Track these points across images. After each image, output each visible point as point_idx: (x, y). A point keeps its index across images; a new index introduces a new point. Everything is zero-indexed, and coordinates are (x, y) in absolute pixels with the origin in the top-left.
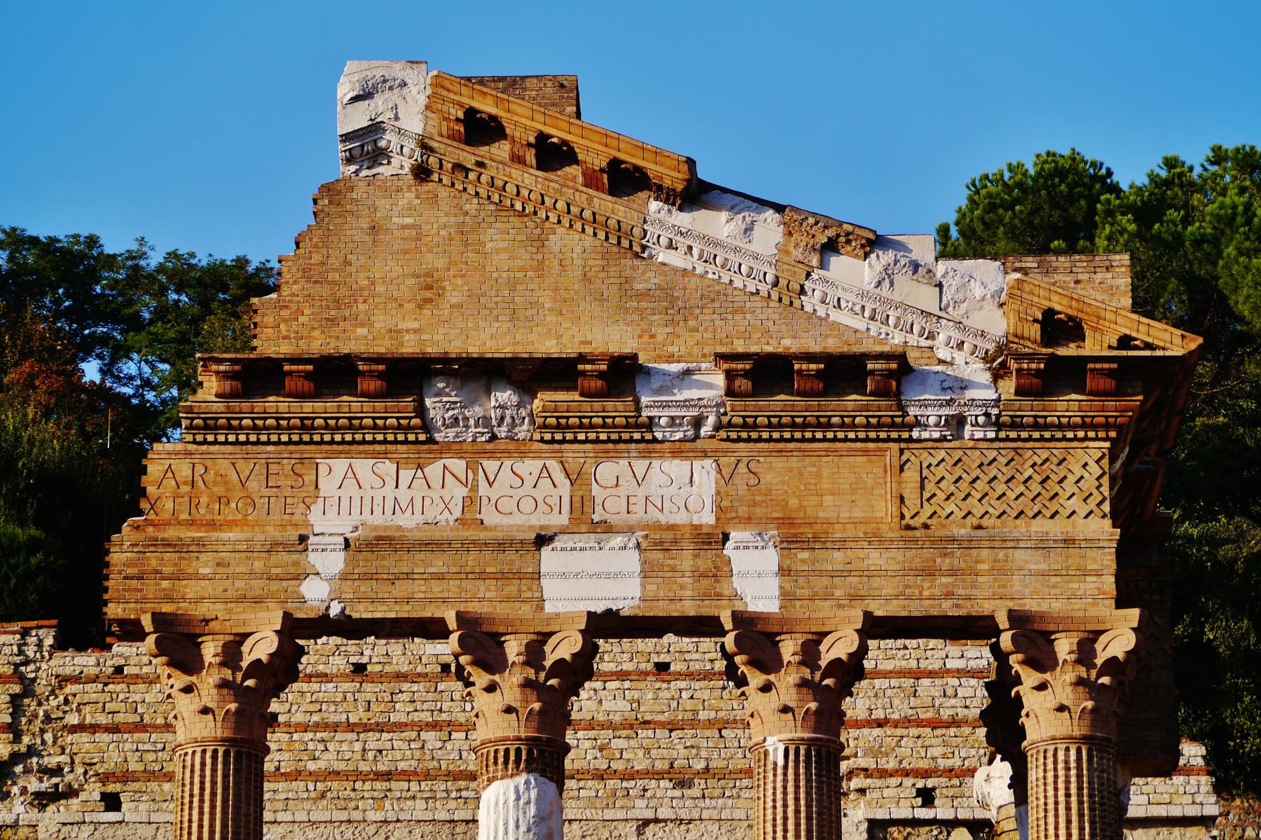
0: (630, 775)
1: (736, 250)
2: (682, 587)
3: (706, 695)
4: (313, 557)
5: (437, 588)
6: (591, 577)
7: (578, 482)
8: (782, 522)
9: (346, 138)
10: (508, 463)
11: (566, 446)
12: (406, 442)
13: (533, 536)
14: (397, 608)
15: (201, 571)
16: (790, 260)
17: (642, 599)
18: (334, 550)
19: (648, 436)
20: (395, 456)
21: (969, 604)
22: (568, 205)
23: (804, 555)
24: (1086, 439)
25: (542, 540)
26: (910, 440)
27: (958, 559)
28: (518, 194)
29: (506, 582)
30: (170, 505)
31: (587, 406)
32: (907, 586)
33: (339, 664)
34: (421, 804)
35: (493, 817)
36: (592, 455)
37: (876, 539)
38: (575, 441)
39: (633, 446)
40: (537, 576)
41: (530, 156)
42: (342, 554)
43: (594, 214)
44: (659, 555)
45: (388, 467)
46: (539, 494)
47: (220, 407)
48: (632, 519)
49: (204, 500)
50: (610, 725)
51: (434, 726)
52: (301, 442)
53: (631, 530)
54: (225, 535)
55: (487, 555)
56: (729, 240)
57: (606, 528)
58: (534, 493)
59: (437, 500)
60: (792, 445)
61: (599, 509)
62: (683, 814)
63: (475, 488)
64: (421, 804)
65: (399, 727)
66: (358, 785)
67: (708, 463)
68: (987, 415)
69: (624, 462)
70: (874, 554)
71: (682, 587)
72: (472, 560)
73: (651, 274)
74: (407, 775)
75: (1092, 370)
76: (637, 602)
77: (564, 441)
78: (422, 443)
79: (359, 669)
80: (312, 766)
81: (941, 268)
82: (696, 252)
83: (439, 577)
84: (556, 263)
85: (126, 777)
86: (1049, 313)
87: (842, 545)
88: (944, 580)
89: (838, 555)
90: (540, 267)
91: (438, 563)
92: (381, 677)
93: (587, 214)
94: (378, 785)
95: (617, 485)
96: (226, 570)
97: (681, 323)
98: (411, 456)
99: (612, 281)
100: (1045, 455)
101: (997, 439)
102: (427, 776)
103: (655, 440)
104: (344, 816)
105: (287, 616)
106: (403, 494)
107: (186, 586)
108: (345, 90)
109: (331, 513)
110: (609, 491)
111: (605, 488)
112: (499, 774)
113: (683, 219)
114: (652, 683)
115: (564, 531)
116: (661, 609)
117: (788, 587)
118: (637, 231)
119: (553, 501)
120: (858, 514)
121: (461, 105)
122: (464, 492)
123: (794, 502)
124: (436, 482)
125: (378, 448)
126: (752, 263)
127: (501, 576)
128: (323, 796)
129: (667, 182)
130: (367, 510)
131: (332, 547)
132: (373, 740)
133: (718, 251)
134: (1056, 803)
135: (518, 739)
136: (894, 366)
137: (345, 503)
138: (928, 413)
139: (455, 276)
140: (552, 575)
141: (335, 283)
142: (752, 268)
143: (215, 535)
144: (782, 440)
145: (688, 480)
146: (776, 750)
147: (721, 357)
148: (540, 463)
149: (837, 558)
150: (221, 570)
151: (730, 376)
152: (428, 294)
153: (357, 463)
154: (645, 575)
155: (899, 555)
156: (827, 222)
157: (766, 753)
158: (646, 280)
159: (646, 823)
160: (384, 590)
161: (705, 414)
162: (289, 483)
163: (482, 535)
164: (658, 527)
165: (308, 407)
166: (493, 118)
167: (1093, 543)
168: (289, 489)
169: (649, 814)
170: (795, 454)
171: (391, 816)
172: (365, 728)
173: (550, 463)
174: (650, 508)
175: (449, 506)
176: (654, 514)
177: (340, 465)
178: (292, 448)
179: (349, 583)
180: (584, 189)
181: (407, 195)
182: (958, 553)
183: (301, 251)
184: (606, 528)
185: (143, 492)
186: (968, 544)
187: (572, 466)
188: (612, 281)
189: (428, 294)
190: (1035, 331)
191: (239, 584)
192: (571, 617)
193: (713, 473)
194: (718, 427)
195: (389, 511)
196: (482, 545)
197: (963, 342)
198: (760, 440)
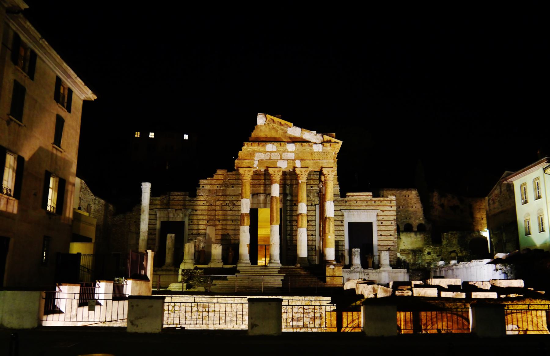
25: (277, 160)
46: (277, 156)
53: (286, 160)
67: (294, 153)
85: (234, 184)
90: (277, 134)
106: (264, 156)
123: (302, 157)
148: (277, 153)
177: (258, 153)
184: (284, 160)
185: (238, 156)
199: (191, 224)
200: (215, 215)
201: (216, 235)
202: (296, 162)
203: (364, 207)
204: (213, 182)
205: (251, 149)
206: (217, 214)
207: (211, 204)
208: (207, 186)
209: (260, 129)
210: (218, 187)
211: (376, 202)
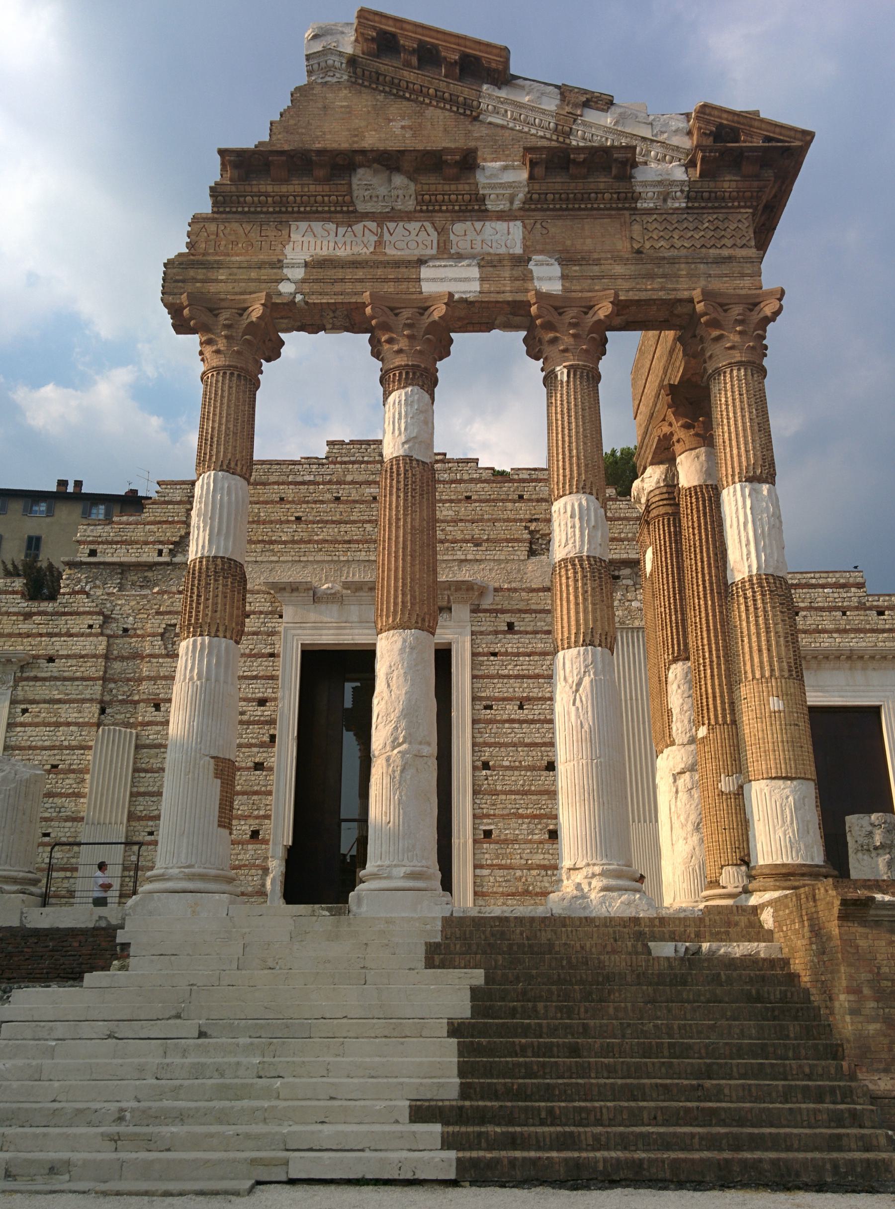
0: (455, 541)
1: (533, 109)
2: (504, 285)
3: (487, 509)
4: (285, 271)
5: (359, 287)
6: (450, 280)
8: (560, 252)
9: (308, 57)
10: (401, 224)
11: (434, 214)
12: (342, 212)
13: (416, 258)
14: (335, 297)
16: (564, 113)
17: (480, 292)
19: (483, 208)
21: (674, 292)
22: (436, 91)
23: (577, 268)
24: (739, 207)
25: (421, 262)
26: (636, 209)
27: (667, 269)
28: (407, 88)
30: (203, 245)
31: (447, 188)
32: (638, 284)
33: (328, 496)
34: (363, 553)
35: (392, 411)
37: (617, 259)
38: (441, 211)
39: (474, 214)
40: (419, 280)
41: (414, 61)
43: (451, 95)
44: (490, 269)
45: (332, 226)
47: (233, 189)
48: (475, 251)
49: (223, 243)
50: (447, 522)
51: (369, 522)
52: (280, 212)
54: (234, 259)
57: (460, 257)
58: (416, 238)
59: (359, 242)
60: (566, 213)
61: (454, 246)
62: (478, 557)
63: (382, 236)
64: (363, 553)
65: (354, 522)
66: (336, 546)
67: (519, 223)
68: (682, 191)
69: (469, 223)
70: (618, 267)
71: (504, 285)
72: (380, 272)
73: (483, 129)
74: (358, 542)
76: (477, 294)
77: (432, 211)
79: (337, 499)
80: (316, 538)
84: (429, 123)
86: (720, 126)
87: (597, 261)
88: (659, 280)
89: (596, 268)
91: (360, 274)
92: (347, 502)
94: (345, 546)
100: (715, 216)
101: (687, 208)
102: (367, 542)
103: (486, 210)
104: (330, 558)
105: (269, 296)
108: (309, 34)
110: (460, 238)
113: (503, 93)
114: (463, 504)
115: (433, 258)
116: (493, 297)
117: (567, 285)
118: (475, 103)
119: (428, 243)
121: (374, 28)
122: (376, 238)
123: (569, 243)
124: (359, 234)
125: (325, 215)
126: (542, 117)
127: (397, 280)
128: (321, 550)
129: (494, 65)
130: (318, 248)
132: (343, 528)
133: (523, 111)
134: (734, 400)
135: (407, 365)
136: (630, 155)
137: (306, 245)
140: (428, 280)
141: (302, 134)
142: (541, 120)
143: (228, 259)
144: (561, 209)
145: (506, 232)
146: (562, 373)
147: (527, 150)
148: (419, 224)
150: (231, 277)
151: (533, 164)
152: (356, 139)
153: (313, 224)
154: (482, 279)
155: (633, 268)
156: (586, 92)
157: (556, 376)
158: (479, 131)
159: (462, 561)
160: (328, 288)
162: (273, 234)
163: (386, 258)
164: (489, 254)
165: (284, 189)
166: (394, 36)
169: (463, 557)
171: (350, 558)
172: (340, 522)
173: (425, 223)
174: (485, 246)
176: (487, 249)
177: (303, 225)
178: (275, 216)
181: (345, 92)
182: (667, 266)
183: (283, 119)
186: (673, 261)
187: (437, 224)
189: (356, 139)
190: (709, 141)
191: (241, 284)
193: (521, 228)
195: (331, 248)
196: (386, 264)
197: (665, 156)
198: (548, 209)
199: (21, 719)
200: (140, 680)
201: (136, 770)
202: (531, 266)
203: (835, 635)
204: (139, 533)
205: (263, 198)
206: (145, 673)
207: (126, 630)
208: (110, 549)
209: (320, 105)
210: (160, 553)
211: (886, 613)
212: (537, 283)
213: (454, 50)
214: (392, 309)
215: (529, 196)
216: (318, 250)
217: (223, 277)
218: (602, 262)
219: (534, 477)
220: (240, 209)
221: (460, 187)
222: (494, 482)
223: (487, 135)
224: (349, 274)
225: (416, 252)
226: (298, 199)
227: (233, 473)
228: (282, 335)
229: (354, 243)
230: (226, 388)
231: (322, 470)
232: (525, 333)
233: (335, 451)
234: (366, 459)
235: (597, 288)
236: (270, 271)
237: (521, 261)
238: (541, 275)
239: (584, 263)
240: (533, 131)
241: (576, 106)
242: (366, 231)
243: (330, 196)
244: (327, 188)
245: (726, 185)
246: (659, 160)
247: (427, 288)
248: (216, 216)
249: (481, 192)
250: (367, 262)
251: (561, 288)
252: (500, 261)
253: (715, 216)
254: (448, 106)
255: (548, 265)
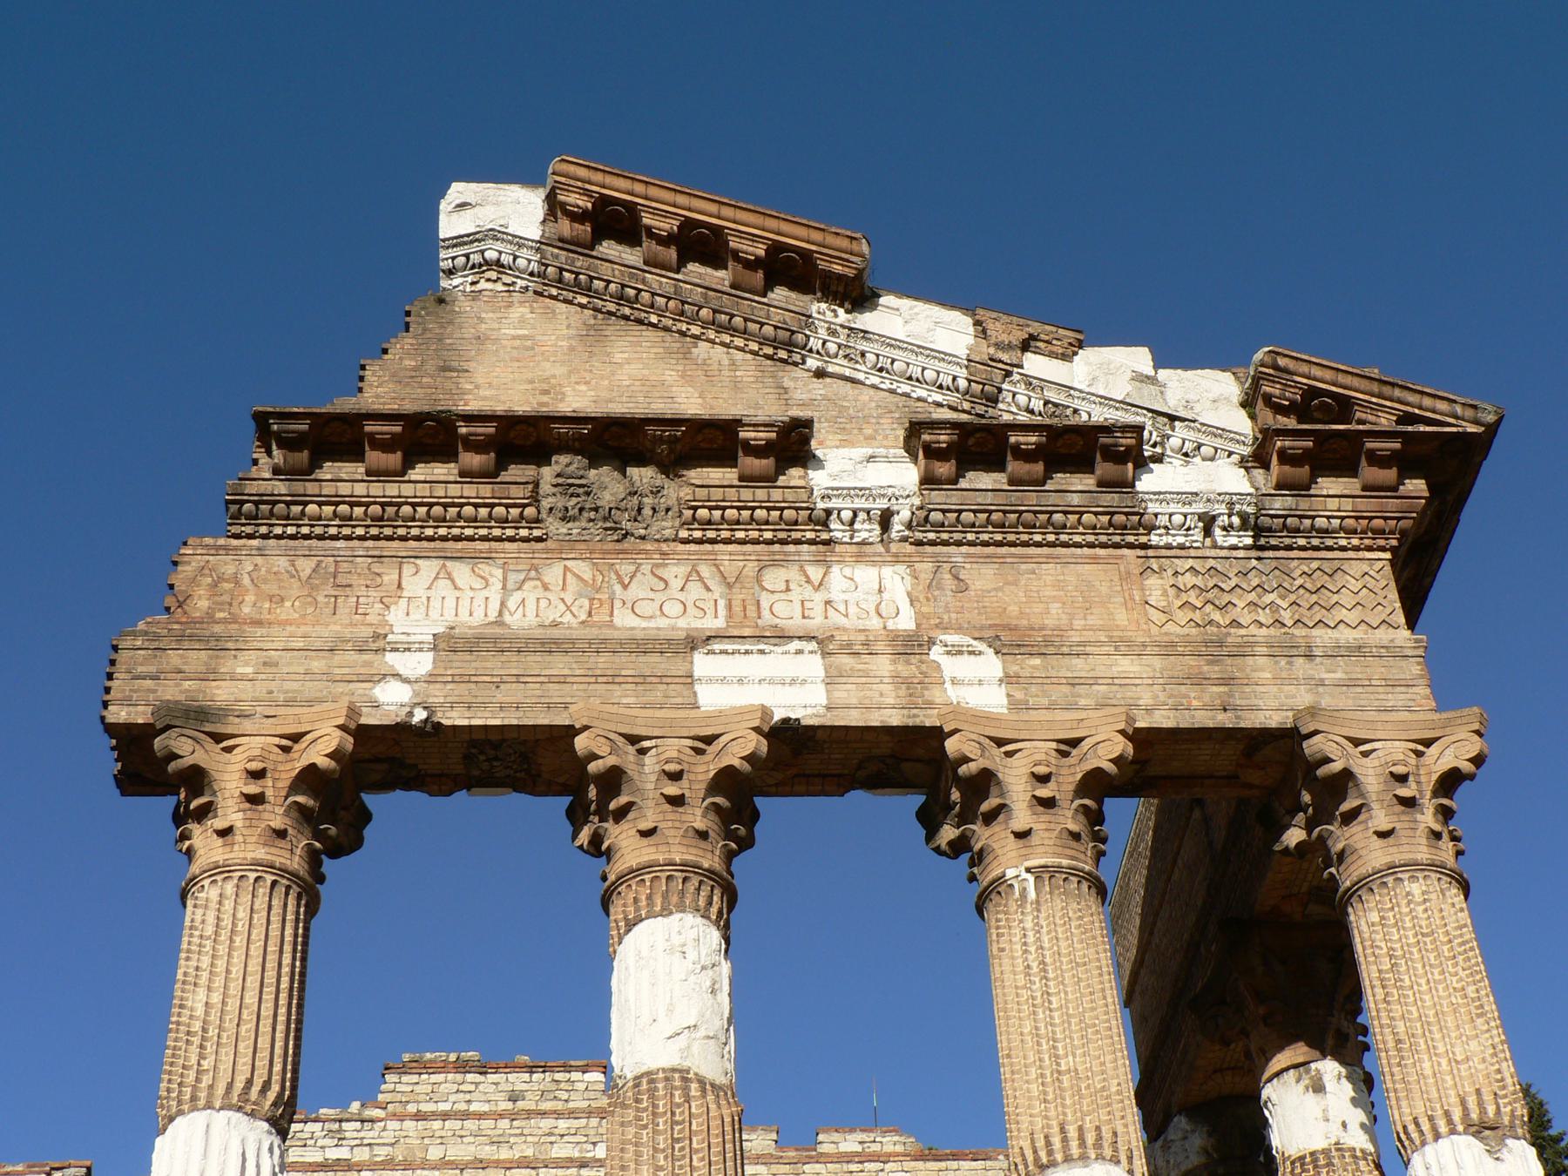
7: (737, 585)
11: (717, 547)
13: (682, 635)
15: (239, 670)
17: (828, 708)
18: (421, 650)
19: (825, 536)
20: (503, 555)
23: (1037, 661)
25: (694, 643)
26: (1145, 546)
29: (648, 687)
36: (753, 558)
37: (1123, 645)
40: (689, 679)
41: (672, 254)
42: (431, 655)
44: (846, 661)
47: (281, 487)
49: (250, 598)
55: (624, 658)
56: (909, 340)
58: (681, 596)
61: (766, 613)
67: (901, 568)
72: (602, 662)
75: (1371, 453)
76: (822, 711)
78: (539, 540)
81: (1163, 374)
82: (871, 357)
83: (562, 680)
88: (1215, 689)
89: (1075, 661)
91: (560, 665)
93: (738, 321)
95: (788, 590)
96: (274, 670)
97: (855, 431)
98: (522, 555)
99: (768, 390)
105: (353, 711)
107: (218, 688)
109: (417, 615)
110: (777, 596)
111: (773, 592)
112: (643, 913)
116: (854, 719)
117: (1019, 695)
119: (709, 606)
120: (1093, 620)
121: (587, 193)
123: (1013, 609)
125: (479, 545)
126: (941, 366)
127: (642, 680)
131: (417, 646)
133: (896, 354)
137: (436, 603)
138: (1171, 511)
139: (577, 383)
140: (710, 681)
149: (1079, 666)
154: (830, 681)
155: (1157, 663)
161: (895, 508)
165: (392, 490)
167: (1392, 652)
168: (363, 588)
170: (1008, 560)
174: (831, 612)
175: (573, 609)
176: (836, 619)
177: (429, 567)
178: (370, 543)
179: (438, 686)
180: (733, 292)
188: (768, 390)
192: (741, 712)
194: (909, 526)
202: (936, 653)
205: (343, 509)
212: (953, 694)
213: (754, 238)
214: (633, 739)
215: (922, 514)
216: (464, 616)
217: (249, 670)
218: (1088, 649)
219: (875, 1148)
220: (291, 530)
221: (776, 494)
222: (779, 1161)
223: (825, 398)
224: (533, 663)
225: (682, 623)
226: (422, 510)
227: (252, 1114)
228: (369, 799)
229: (543, 603)
230: (242, 914)
231: (369, 1134)
232: (924, 798)
233: (399, 1088)
234: (474, 1107)
235: (1083, 702)
236: (353, 656)
237: (912, 646)
238: (959, 675)
239: (1051, 650)
240: (920, 392)
241: (1009, 347)
242: (569, 575)
243: (492, 506)
244: (486, 490)
245: (1333, 504)
246: (1186, 455)
247: (711, 698)
248: (235, 542)
249: (821, 505)
250: (573, 641)
251: (1005, 701)
252: (866, 644)
253: (1315, 565)
254: (739, 342)
255: (970, 653)
